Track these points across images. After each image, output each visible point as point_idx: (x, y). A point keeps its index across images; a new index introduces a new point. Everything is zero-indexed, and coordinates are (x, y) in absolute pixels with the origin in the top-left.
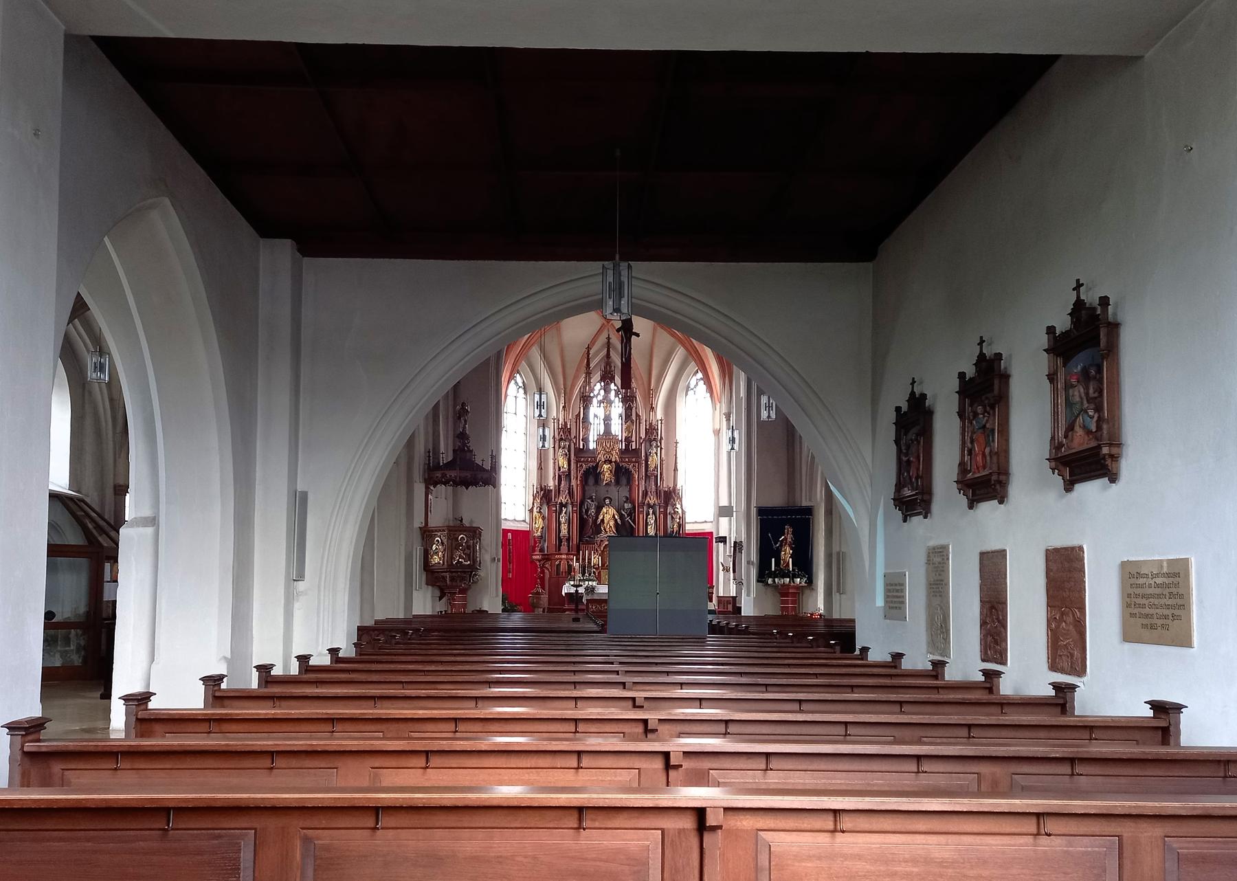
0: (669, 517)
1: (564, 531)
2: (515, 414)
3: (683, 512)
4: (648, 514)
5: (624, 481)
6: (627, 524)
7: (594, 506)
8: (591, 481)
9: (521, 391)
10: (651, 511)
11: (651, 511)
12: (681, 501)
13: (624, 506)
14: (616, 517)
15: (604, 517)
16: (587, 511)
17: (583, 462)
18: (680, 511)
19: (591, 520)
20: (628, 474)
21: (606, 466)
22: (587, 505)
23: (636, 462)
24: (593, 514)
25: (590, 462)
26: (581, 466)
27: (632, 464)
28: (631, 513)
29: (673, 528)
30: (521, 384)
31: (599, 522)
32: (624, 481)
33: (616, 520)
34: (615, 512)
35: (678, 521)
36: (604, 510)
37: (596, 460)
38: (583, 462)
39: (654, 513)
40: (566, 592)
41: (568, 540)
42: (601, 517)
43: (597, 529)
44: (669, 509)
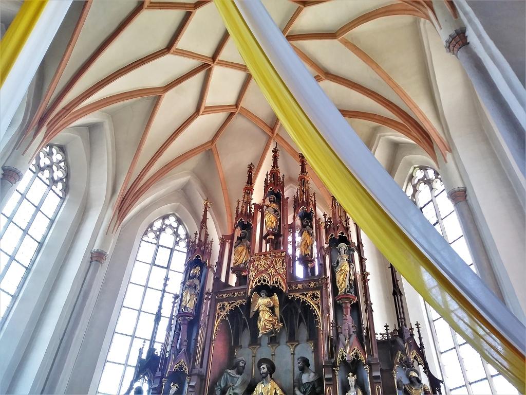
5: (303, 332)
8: (245, 338)
9: (183, 246)
10: (352, 380)
11: (352, 380)
12: (422, 355)
13: (300, 379)
17: (226, 299)
18: (425, 380)
20: (308, 315)
21: (262, 302)
23: (317, 289)
25: (239, 298)
26: (223, 307)
27: (310, 293)
30: (183, 237)
32: (303, 332)
37: (246, 293)
38: (226, 299)
44: (399, 375)
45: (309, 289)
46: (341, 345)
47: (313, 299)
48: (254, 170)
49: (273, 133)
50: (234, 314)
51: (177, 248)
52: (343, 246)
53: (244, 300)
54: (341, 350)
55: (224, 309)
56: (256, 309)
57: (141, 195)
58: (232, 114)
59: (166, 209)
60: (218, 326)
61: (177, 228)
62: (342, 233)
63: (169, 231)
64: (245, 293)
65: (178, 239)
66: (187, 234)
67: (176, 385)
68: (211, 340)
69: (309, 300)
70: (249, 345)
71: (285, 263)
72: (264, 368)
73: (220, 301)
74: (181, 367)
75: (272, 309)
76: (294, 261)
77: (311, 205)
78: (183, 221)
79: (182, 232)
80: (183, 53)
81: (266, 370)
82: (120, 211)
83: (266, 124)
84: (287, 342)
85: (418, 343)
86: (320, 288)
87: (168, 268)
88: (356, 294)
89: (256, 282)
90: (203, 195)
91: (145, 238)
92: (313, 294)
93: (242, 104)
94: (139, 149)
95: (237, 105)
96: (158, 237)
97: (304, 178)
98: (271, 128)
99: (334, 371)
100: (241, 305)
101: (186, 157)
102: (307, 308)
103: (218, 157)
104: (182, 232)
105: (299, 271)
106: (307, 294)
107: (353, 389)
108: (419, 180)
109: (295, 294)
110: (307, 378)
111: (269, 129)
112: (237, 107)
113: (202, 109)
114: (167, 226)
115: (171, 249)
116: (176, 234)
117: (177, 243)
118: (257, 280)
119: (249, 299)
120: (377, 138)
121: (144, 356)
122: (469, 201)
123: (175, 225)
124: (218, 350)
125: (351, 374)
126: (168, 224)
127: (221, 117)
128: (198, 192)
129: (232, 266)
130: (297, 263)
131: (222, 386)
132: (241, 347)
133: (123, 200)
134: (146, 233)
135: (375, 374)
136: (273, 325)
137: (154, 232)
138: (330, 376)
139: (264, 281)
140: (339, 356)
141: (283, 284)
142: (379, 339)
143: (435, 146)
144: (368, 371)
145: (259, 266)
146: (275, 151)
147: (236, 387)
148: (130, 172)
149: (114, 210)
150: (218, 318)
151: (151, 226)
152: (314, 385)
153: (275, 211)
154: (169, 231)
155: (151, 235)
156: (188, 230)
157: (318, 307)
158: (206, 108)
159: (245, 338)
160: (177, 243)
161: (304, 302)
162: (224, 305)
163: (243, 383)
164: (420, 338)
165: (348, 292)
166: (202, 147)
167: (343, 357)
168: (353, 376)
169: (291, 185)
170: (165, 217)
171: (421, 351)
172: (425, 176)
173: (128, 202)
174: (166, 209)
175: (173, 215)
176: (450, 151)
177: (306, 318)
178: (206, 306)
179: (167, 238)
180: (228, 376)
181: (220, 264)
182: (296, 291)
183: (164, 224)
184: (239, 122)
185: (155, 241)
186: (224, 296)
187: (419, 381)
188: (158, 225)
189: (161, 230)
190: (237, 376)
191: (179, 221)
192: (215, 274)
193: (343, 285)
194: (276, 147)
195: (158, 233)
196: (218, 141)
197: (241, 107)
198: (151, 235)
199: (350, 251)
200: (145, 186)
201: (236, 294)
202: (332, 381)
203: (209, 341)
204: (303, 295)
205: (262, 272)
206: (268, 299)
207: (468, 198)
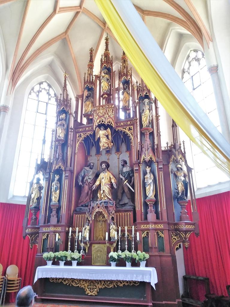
0: (172, 176)
1: (55, 198)
2: (46, 114)
3: (189, 169)
4: (145, 173)
5: (124, 147)
6: (126, 190)
7: (91, 173)
8: (93, 151)
9: (53, 101)
11: (148, 170)
12: (184, 157)
13: (122, 170)
14: (113, 181)
15: (100, 184)
16: (83, 178)
18: (185, 169)
19: (86, 187)
20: (126, 139)
21: (101, 133)
22: (84, 172)
23: (132, 125)
24: (89, 181)
25: (88, 131)
26: (80, 136)
27: (128, 127)
28: (130, 177)
29: (177, 189)
30: (53, 95)
31: (94, 187)
32: (124, 147)
33: (112, 185)
34: (112, 177)
35: (183, 178)
36: (102, 175)
39: (152, 172)
40: (40, 277)
41: (59, 209)
42: (97, 183)
43: (94, 193)
44: (172, 166)
45: (127, 125)
46: (143, 153)
47: (129, 130)
48: (94, 52)
49: (105, 26)
50: (86, 139)
51: (50, 102)
52: (146, 101)
53: (91, 132)
54: (143, 156)
55: (81, 137)
56: (98, 136)
57: (24, 70)
58: (77, 13)
59: (41, 78)
60: (78, 146)
61: (49, 90)
62: (146, 93)
63: (44, 93)
64: (92, 128)
65: (50, 97)
66: (55, 94)
67: (58, 176)
68: (75, 153)
69: (127, 131)
70: (96, 155)
71: (114, 112)
72: (103, 166)
73: (78, 132)
74: (60, 167)
75: (107, 136)
76: (119, 108)
77: (129, 75)
78: (51, 85)
79: (52, 92)
80: (65, 9)
81: (105, 167)
82: (13, 80)
83: (100, 20)
84: (115, 153)
85: (183, 151)
86: (133, 125)
87: (46, 114)
88: (153, 127)
89: (98, 123)
90: (63, 69)
91: (30, 96)
92: (129, 128)
93: (84, 6)
94: (19, 39)
95: (80, 6)
96: (38, 96)
97: (125, 58)
98: (104, 23)
99: (139, 166)
100: (90, 135)
101: (50, 44)
102: (125, 135)
103: (70, 43)
104: (52, 92)
105: (122, 115)
106: (126, 128)
107: (148, 174)
108: (193, 59)
109: (119, 128)
110: (126, 169)
111: (103, 24)
112: (81, 8)
113: (58, 9)
114: (42, 89)
115: (47, 103)
116: (48, 94)
117: (50, 99)
118: (98, 121)
119: (95, 131)
120: (170, 30)
121: (39, 162)
122: (219, 73)
123: (47, 88)
124: (79, 158)
125: (148, 167)
126: (43, 88)
127: (71, 14)
128: (59, 67)
129: (83, 113)
130: (121, 110)
131: (83, 175)
132: (91, 156)
133: (14, 73)
134: (30, 94)
135: (160, 167)
136: (108, 145)
137: (35, 93)
138: (137, 168)
139: (103, 121)
140: (142, 159)
141: (113, 123)
142: (163, 149)
143: (203, 38)
144: (156, 165)
145: (99, 114)
146: (107, 39)
147: (90, 175)
148: (15, 55)
149: (9, 80)
150: (78, 142)
151: (33, 89)
152: (129, 173)
153: (108, 80)
154: (44, 93)
155: (34, 95)
156: (55, 91)
157: (132, 134)
158: (60, 8)
159: (93, 151)
160: (50, 99)
161: (124, 132)
162: (80, 135)
163: (93, 173)
164: (184, 148)
165: (148, 126)
166: (60, 37)
167: (144, 159)
168: (149, 168)
169: (117, 62)
170: (41, 83)
171: (184, 155)
172: (196, 56)
173: (17, 75)
174: (41, 78)
175: (46, 82)
176: (212, 41)
177: (125, 140)
178: (71, 135)
179: (44, 96)
180: (85, 170)
181: (76, 112)
182: (119, 126)
183: (40, 88)
184: (82, 18)
185: (37, 98)
186: (81, 130)
187: (181, 169)
188: (37, 88)
189: (39, 92)
190: (90, 170)
191: (49, 86)
192: (74, 118)
193: (145, 123)
194: (107, 37)
195: (37, 93)
196: (69, 32)
197: (84, 8)
198: (34, 95)
199: (150, 103)
200: (26, 64)
201: (87, 129)
202: (138, 171)
203: (74, 154)
204: (124, 128)
205: (101, 117)
206: (105, 131)
207: (218, 71)
